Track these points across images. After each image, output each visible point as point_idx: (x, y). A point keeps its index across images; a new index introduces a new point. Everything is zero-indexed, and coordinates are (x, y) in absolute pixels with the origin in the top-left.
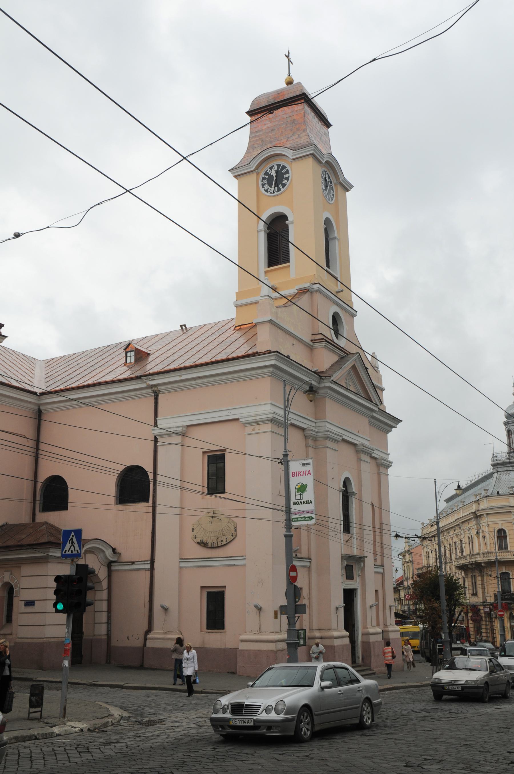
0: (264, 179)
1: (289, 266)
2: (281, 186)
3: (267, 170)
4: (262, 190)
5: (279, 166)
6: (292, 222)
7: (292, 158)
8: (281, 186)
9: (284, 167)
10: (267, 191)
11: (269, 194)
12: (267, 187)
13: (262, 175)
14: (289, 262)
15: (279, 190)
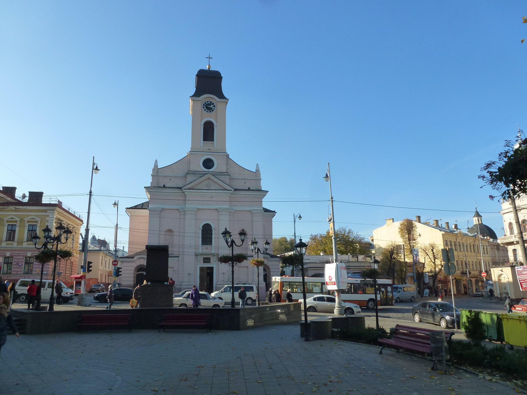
0: (204, 105)
1: (214, 143)
2: (211, 111)
3: (206, 102)
4: (203, 109)
5: (211, 102)
6: (217, 126)
7: (218, 101)
8: (211, 111)
9: (213, 104)
10: (205, 110)
11: (206, 112)
12: (205, 108)
13: (204, 103)
14: (213, 141)
15: (210, 112)
